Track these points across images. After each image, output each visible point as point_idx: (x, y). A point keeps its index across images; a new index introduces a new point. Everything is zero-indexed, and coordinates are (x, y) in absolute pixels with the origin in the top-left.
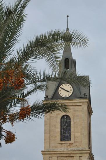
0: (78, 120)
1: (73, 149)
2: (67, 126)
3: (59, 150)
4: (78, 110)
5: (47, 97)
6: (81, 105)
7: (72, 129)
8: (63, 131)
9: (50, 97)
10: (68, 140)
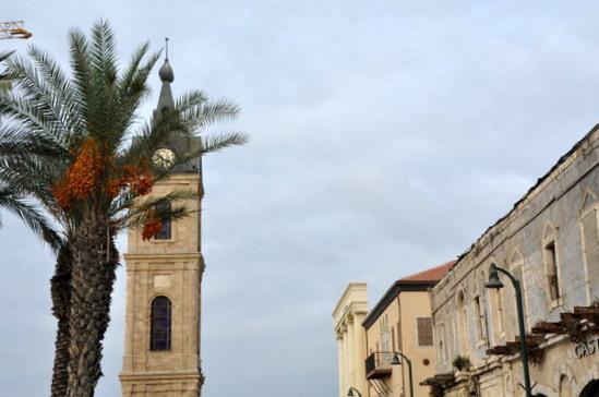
1: (175, 251)
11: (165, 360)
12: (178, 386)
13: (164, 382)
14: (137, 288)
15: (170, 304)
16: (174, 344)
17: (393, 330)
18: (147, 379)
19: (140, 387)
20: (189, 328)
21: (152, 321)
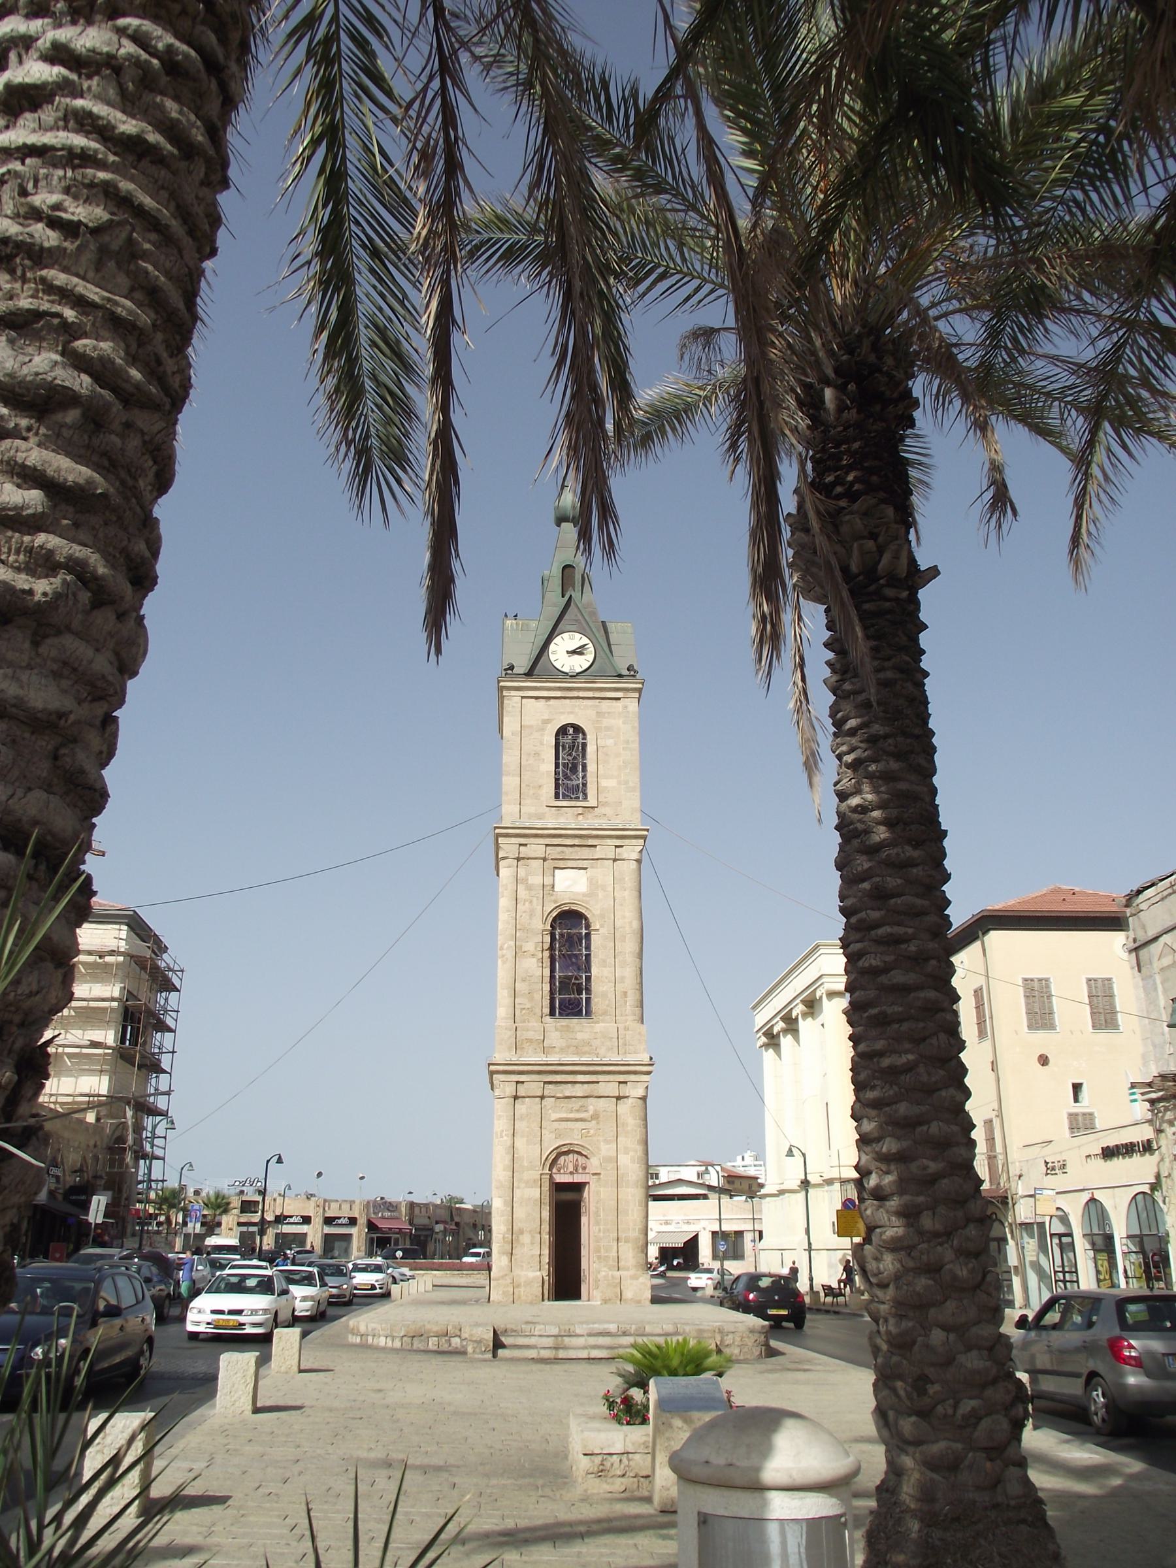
2: (575, 758)
5: (512, 668)
6: (619, 699)
7: (591, 768)
9: (520, 669)
11: (579, 1036)
12: (608, 1086)
13: (580, 1078)
14: (522, 893)
15: (588, 926)
16: (597, 1003)
18: (546, 1072)
19: (533, 1085)
20: (628, 973)
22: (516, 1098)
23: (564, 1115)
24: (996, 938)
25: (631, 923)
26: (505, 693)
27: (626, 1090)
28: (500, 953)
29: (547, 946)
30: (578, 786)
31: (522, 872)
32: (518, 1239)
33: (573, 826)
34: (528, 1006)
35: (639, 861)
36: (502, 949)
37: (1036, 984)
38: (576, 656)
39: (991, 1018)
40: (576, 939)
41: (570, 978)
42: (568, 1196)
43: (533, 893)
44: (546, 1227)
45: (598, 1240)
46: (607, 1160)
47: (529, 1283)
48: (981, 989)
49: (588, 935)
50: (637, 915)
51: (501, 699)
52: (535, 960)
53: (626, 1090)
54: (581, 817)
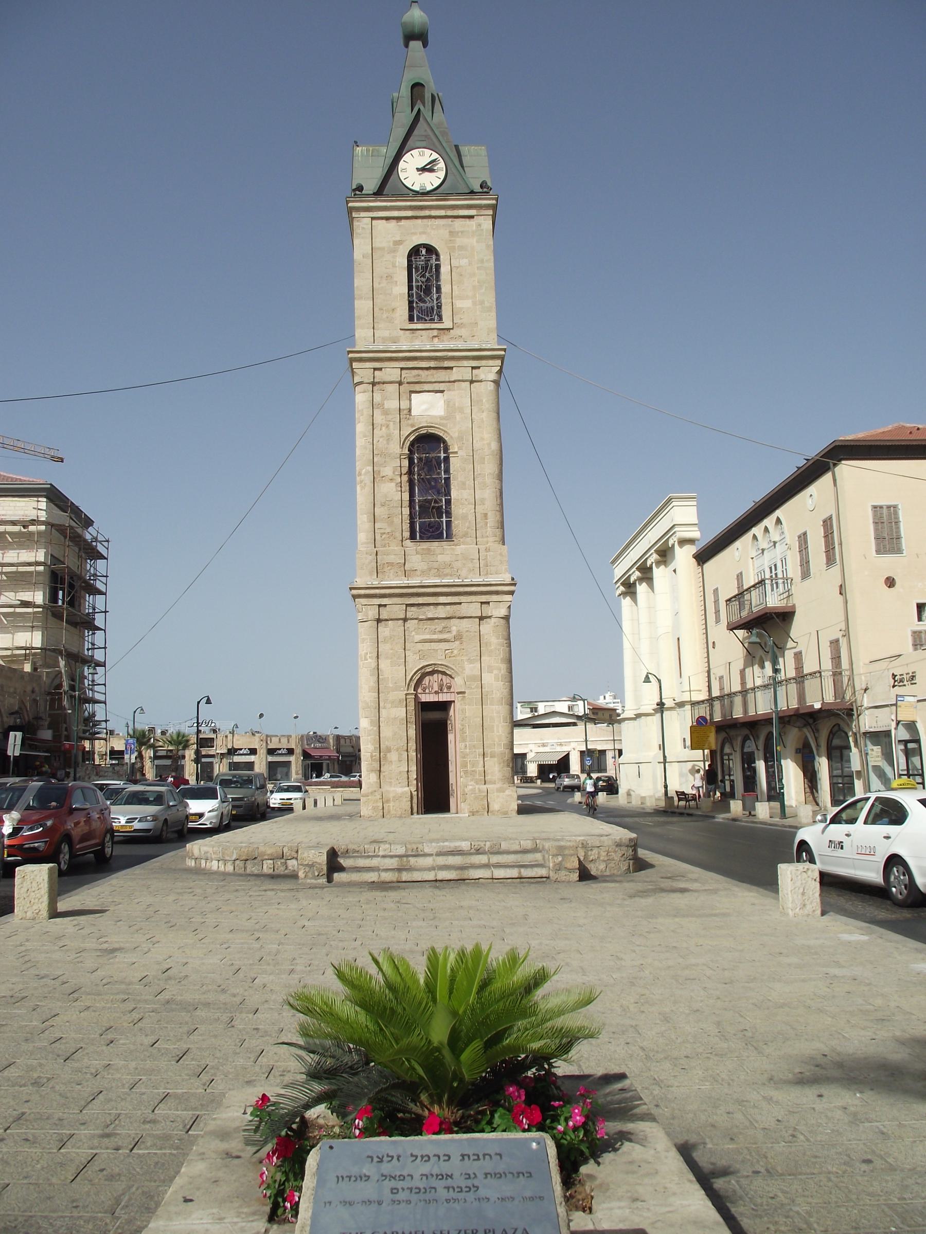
0: (464, 262)
3: (404, 348)
4: (462, 232)
6: (472, 217)
7: (445, 289)
8: (417, 293)
10: (431, 320)
12: (471, 607)
13: (442, 599)
14: (379, 418)
16: (458, 526)
17: (803, 538)
20: (488, 495)
21: (411, 483)
22: (379, 621)
23: (428, 637)
24: (847, 469)
25: (489, 444)
26: (354, 215)
27: (488, 610)
28: (358, 479)
29: (405, 470)
30: (432, 308)
31: (378, 397)
32: (385, 757)
33: (428, 348)
34: (388, 530)
35: (497, 383)
36: (360, 474)
37: (885, 510)
38: (427, 174)
39: (841, 544)
40: (434, 462)
41: (429, 502)
42: (435, 715)
43: (390, 417)
44: (413, 745)
45: (464, 756)
46: (472, 678)
47: (397, 798)
48: (830, 518)
49: (447, 459)
50: (496, 437)
51: (351, 220)
52: (393, 485)
53: (488, 610)
54: (436, 340)
